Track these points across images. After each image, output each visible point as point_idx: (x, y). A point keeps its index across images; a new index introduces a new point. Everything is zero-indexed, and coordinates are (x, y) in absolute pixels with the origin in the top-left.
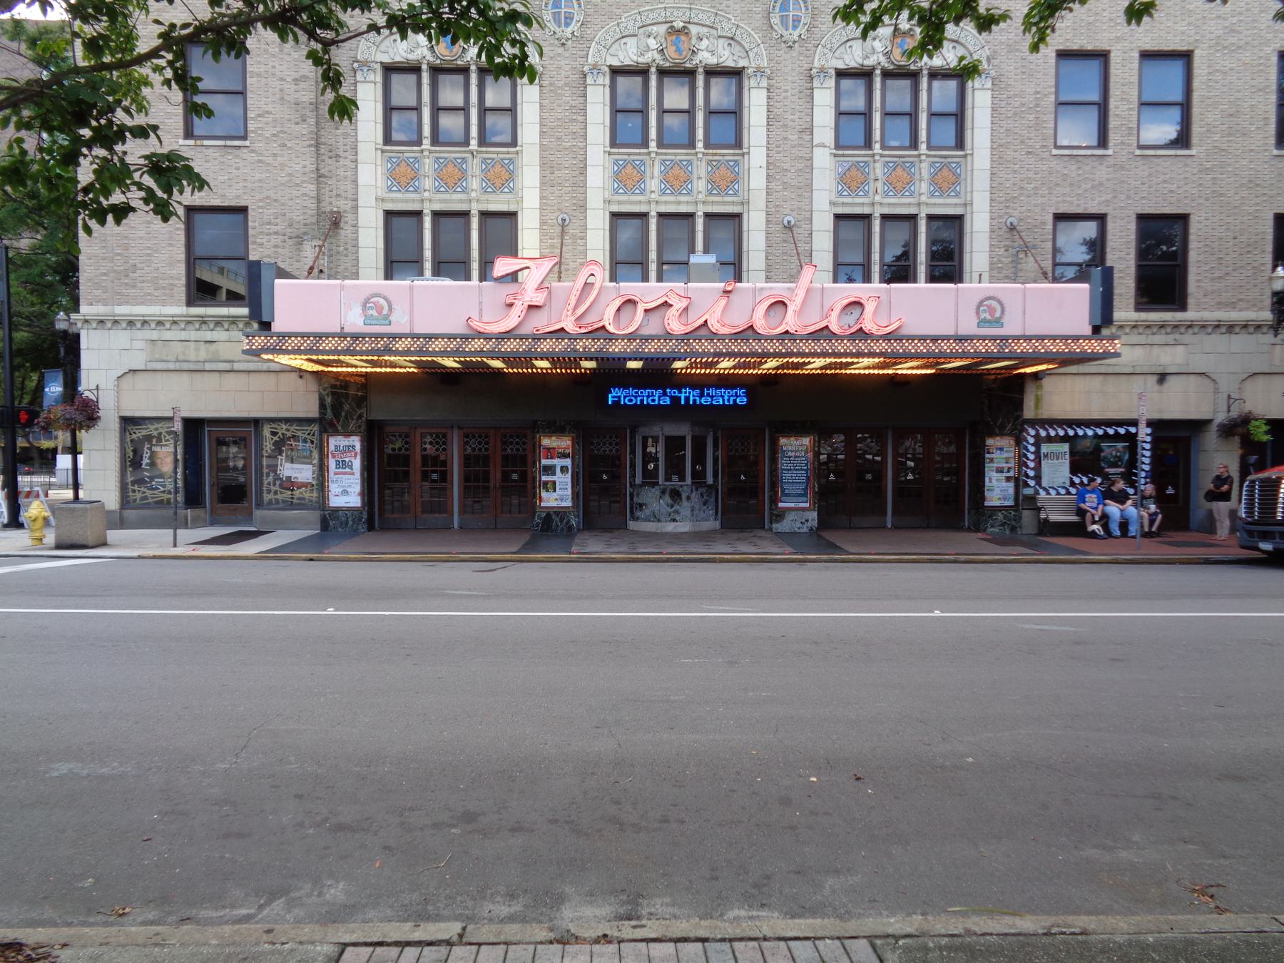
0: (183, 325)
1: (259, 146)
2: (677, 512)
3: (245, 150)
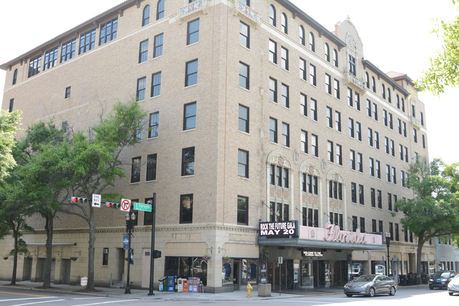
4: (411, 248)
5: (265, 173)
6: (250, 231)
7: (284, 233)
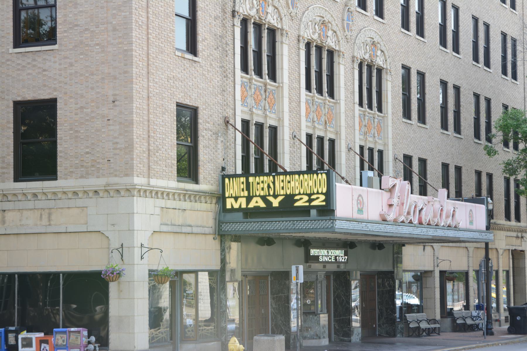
4: (517, 237)
5: (230, 42)
6: (202, 198)
7: (297, 204)
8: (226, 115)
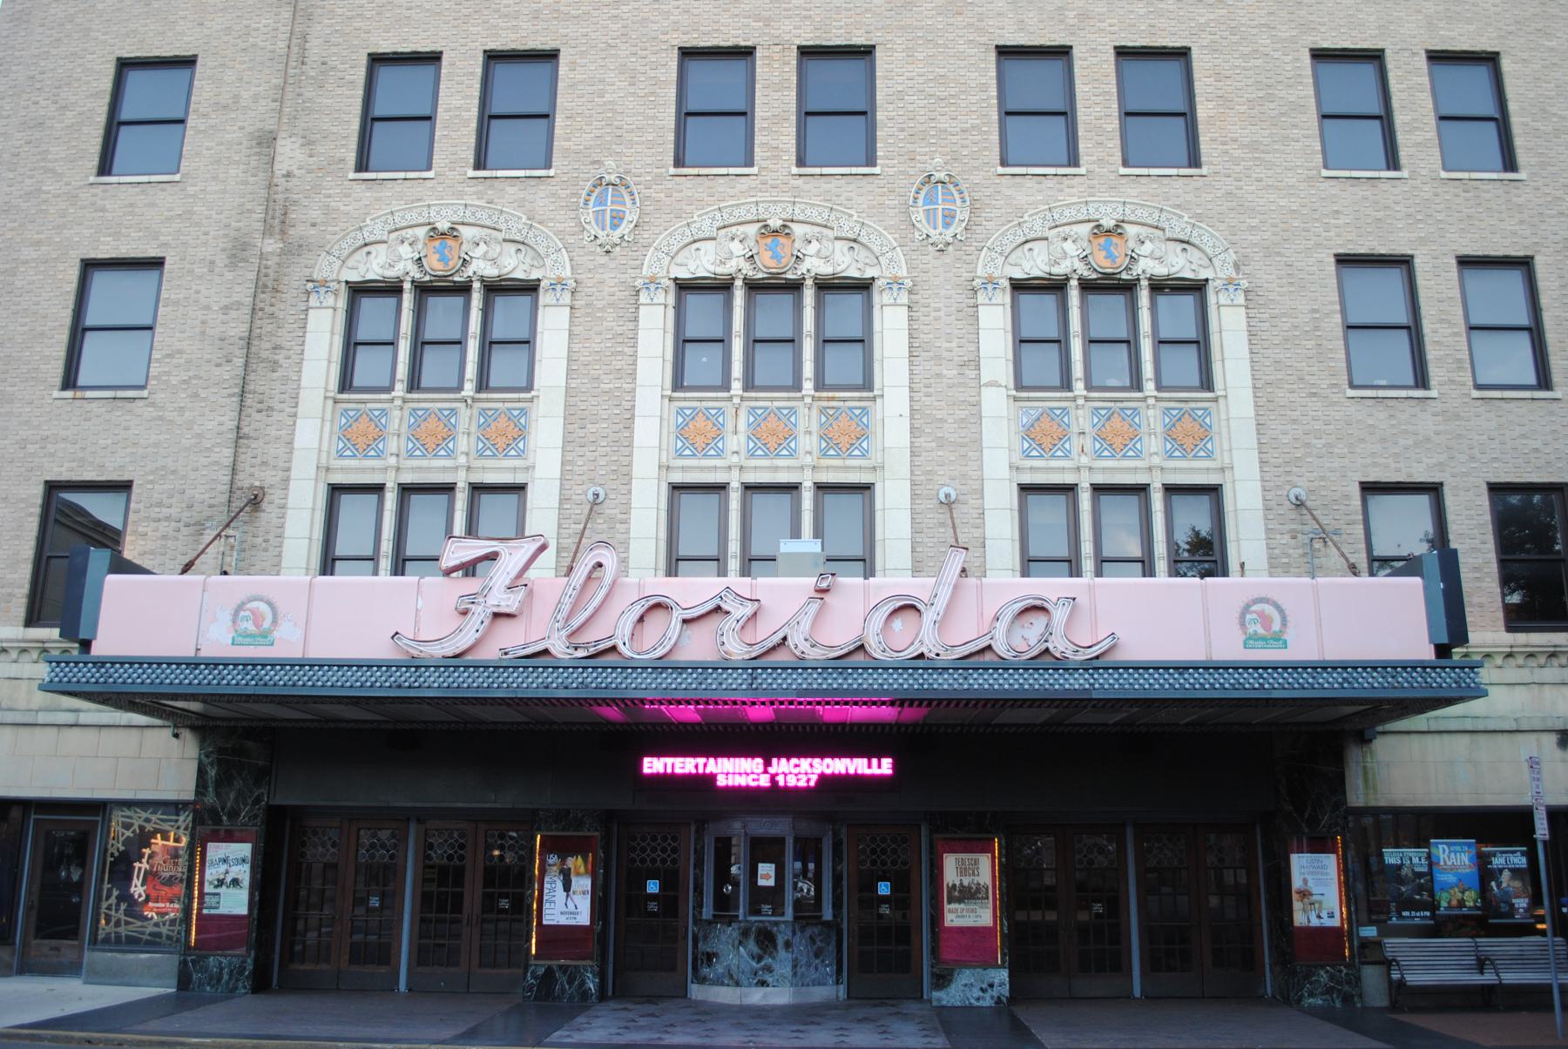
0: (14, 655)
1: (160, 397)
2: (769, 969)
3: (140, 403)
8: (257, 484)
